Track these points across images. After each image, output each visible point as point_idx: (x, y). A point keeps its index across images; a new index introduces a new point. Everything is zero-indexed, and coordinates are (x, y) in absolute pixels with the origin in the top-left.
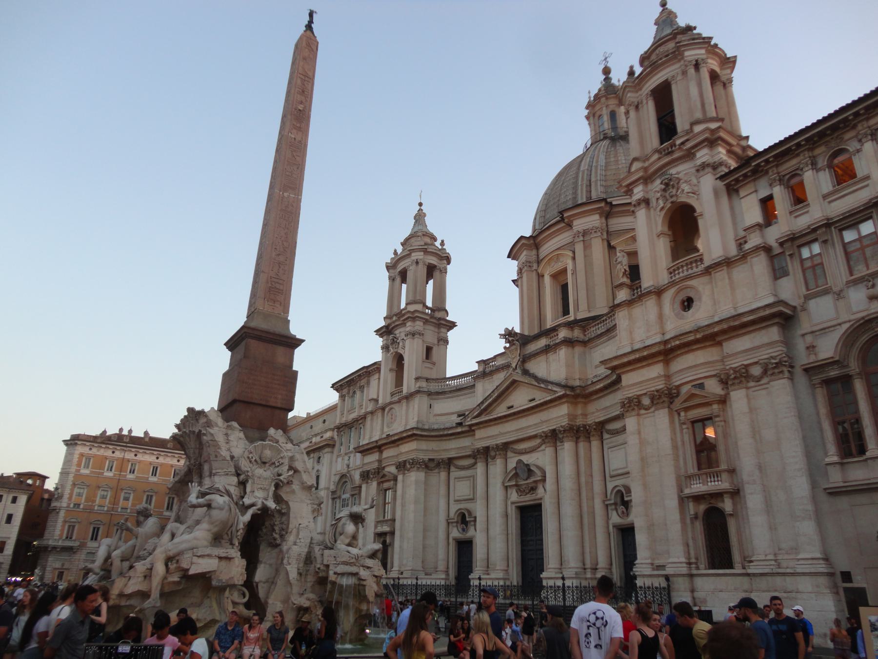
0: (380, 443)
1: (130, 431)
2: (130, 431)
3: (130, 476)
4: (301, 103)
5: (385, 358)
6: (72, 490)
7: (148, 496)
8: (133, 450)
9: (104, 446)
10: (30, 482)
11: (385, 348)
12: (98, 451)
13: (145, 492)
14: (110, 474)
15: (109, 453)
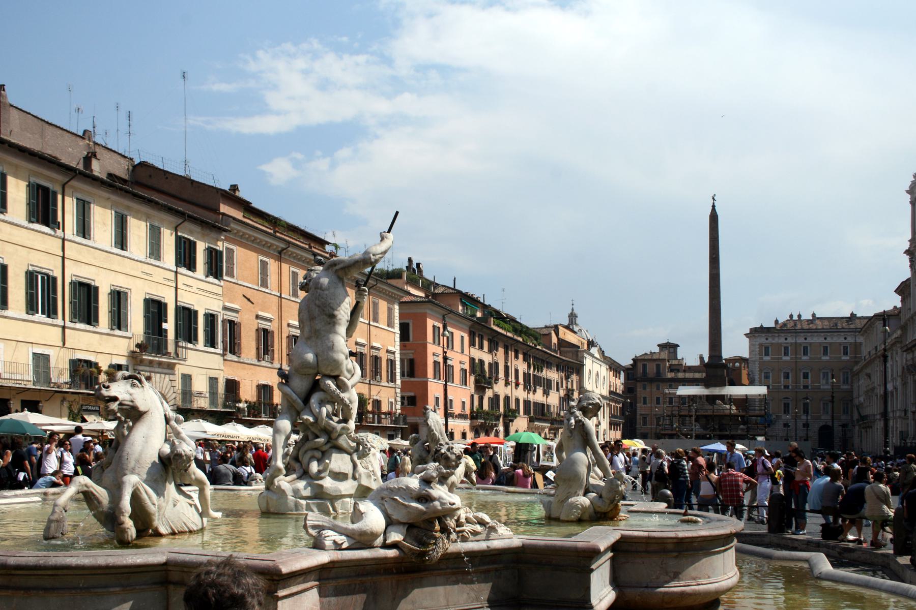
0: (909, 346)
1: (799, 316)
2: (799, 316)
3: (805, 358)
4: (714, 254)
5: (912, 275)
6: (760, 375)
7: (824, 373)
8: (802, 334)
9: (777, 335)
10: (737, 364)
11: (911, 266)
12: (773, 339)
13: (820, 370)
14: (787, 358)
15: (782, 340)
